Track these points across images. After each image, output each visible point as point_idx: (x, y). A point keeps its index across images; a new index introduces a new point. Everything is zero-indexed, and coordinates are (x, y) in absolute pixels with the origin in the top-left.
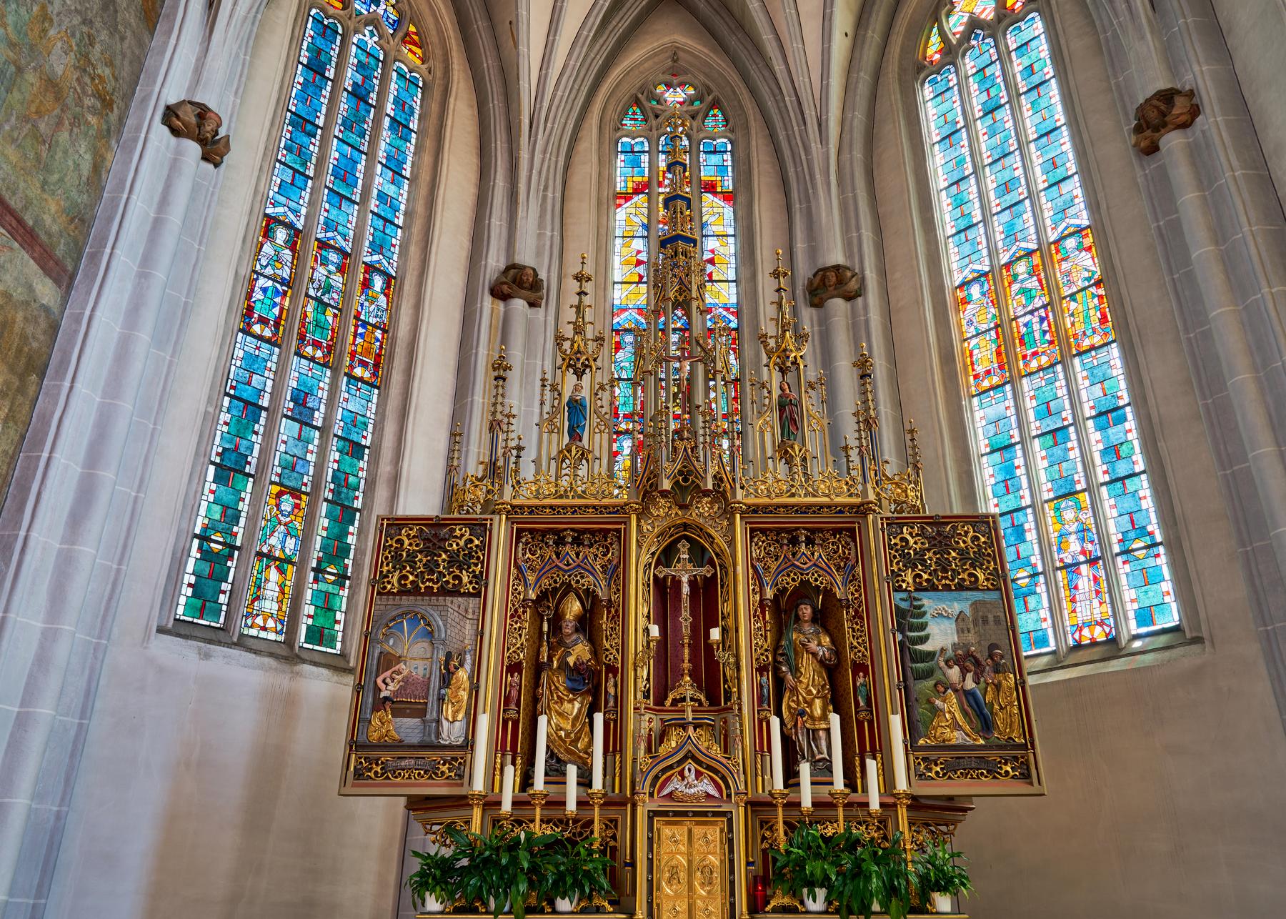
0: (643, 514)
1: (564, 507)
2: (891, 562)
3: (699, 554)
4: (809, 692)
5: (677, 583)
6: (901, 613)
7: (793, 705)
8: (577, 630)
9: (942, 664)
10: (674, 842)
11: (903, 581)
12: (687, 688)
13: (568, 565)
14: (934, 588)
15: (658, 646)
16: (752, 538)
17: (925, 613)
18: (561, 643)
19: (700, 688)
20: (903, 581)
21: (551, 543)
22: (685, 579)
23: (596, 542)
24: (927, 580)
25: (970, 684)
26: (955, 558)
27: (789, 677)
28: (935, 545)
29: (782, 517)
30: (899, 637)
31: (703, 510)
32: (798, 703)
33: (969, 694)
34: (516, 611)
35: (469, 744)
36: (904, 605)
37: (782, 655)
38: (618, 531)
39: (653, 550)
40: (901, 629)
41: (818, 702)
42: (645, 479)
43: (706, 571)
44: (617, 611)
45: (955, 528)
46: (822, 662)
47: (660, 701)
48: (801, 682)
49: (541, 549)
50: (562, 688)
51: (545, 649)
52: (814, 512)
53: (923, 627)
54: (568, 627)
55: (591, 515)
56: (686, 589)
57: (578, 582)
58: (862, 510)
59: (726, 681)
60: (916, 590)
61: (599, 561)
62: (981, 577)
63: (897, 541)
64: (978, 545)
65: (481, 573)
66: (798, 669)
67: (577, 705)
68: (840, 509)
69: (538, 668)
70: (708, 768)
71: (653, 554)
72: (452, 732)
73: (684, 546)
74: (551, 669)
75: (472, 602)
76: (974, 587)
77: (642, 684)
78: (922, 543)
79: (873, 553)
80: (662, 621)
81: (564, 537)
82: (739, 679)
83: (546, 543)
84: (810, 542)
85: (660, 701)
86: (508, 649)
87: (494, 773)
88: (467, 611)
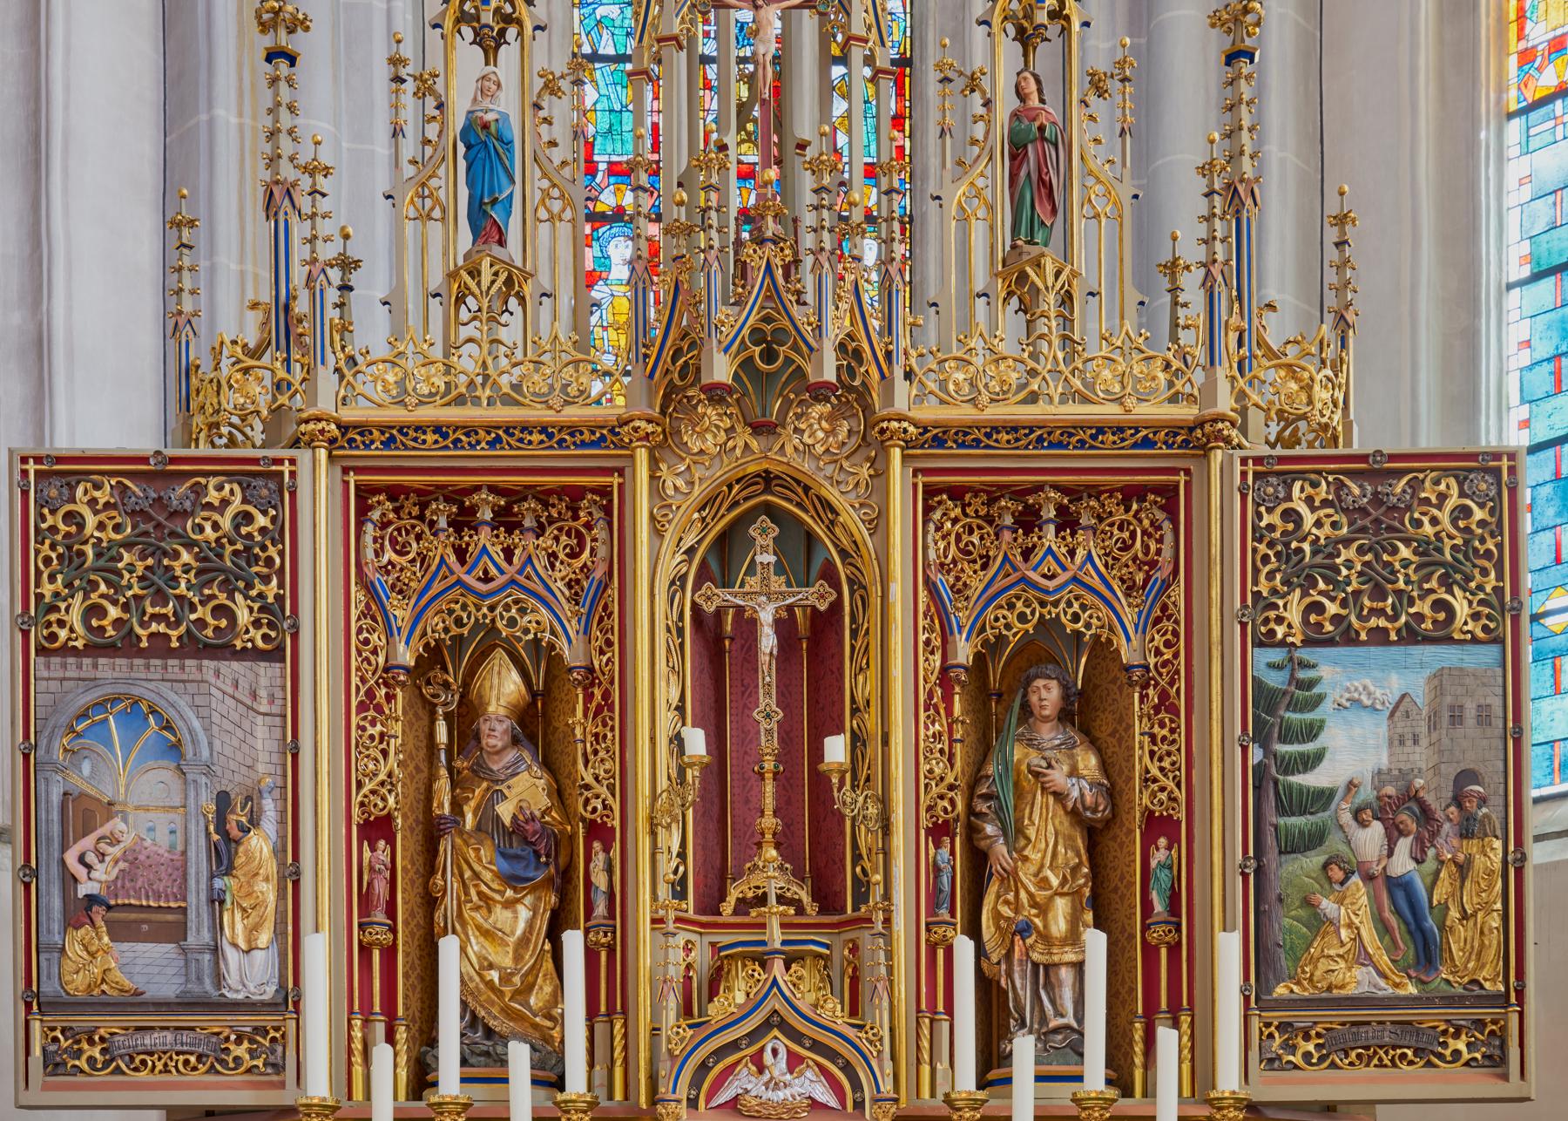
1: (470, 430)
2: (1256, 571)
4: (1044, 883)
6: (1266, 699)
7: (1006, 911)
8: (515, 741)
11: (1280, 620)
13: (487, 579)
14: (1349, 638)
15: (704, 780)
16: (928, 510)
17: (1320, 698)
18: (480, 770)
19: (798, 874)
20: (1280, 620)
21: (443, 523)
22: (766, 616)
23: (551, 521)
24: (1337, 619)
26: (1406, 564)
27: (1001, 848)
28: (1363, 530)
29: (1002, 458)
30: (1256, 755)
32: (1017, 907)
34: (370, 694)
36: (1275, 680)
37: (987, 797)
38: (604, 492)
39: (689, 541)
40: (1261, 735)
41: (1061, 906)
42: (667, 355)
43: (816, 596)
44: (606, 695)
45: (1416, 485)
46: (1074, 814)
47: (710, 903)
48: (1025, 859)
49: (419, 538)
50: (487, 876)
51: (443, 785)
52: (1082, 443)
53: (1311, 731)
55: (536, 453)
56: (768, 641)
57: (512, 622)
59: (857, 858)
60: (1308, 642)
61: (562, 571)
62: (1462, 608)
63: (1275, 519)
64: (1467, 530)
65: (279, 598)
66: (1020, 831)
67: (524, 913)
68: (1144, 436)
69: (432, 832)
71: (691, 551)
73: (764, 531)
74: (461, 833)
75: (267, 673)
77: (667, 866)
78: (1334, 525)
79: (1216, 551)
80: (715, 722)
81: (473, 510)
82: (887, 853)
83: (432, 524)
84: (1067, 522)
85: (710, 903)
86: (360, 785)
88: (254, 696)
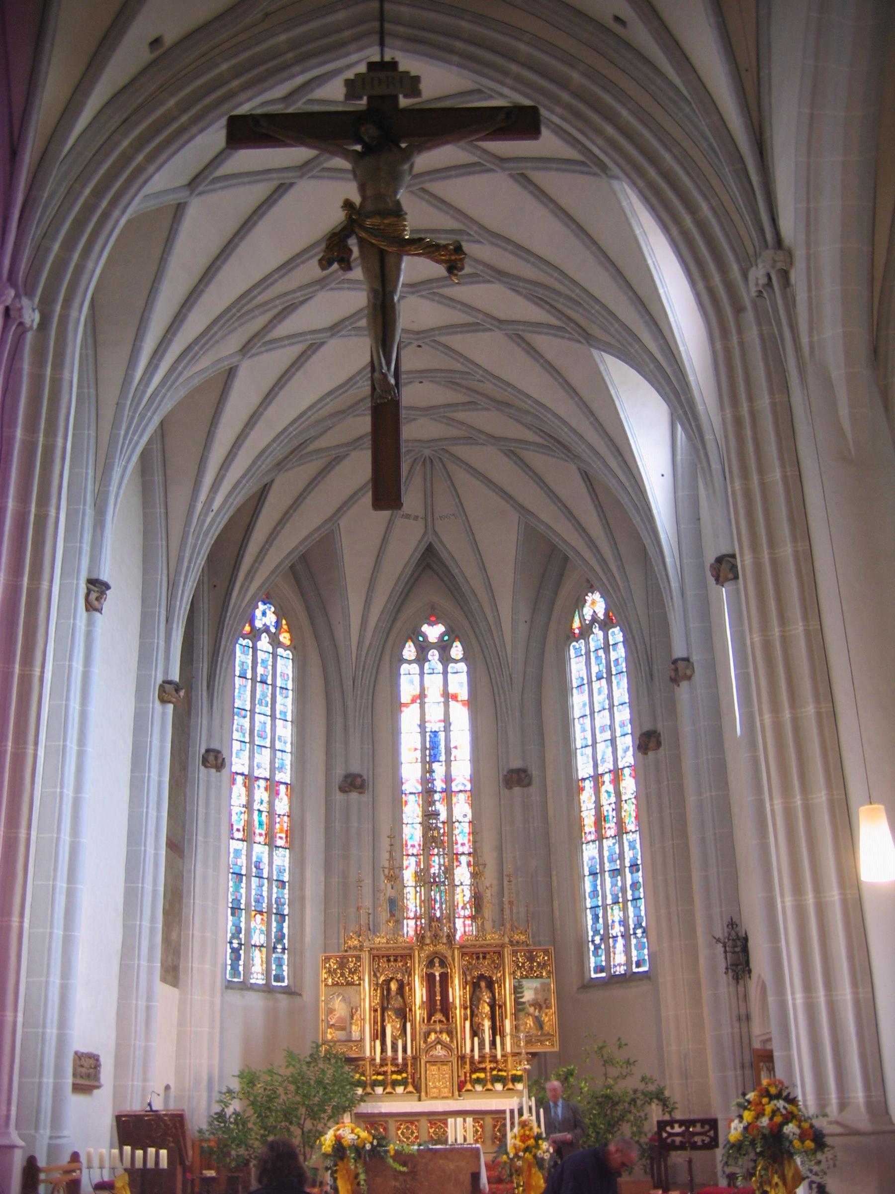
0: (421, 948)
3: (443, 964)
5: (435, 976)
6: (515, 988)
8: (397, 994)
9: (528, 1006)
10: (433, 1070)
12: (439, 1016)
14: (527, 977)
22: (437, 974)
25: (537, 1013)
31: (442, 948)
33: (536, 1017)
35: (362, 1040)
53: (522, 992)
54: (393, 993)
56: (438, 978)
58: (503, 946)
70: (445, 1046)
72: (356, 1035)
76: (542, 977)
87: (373, 1048)
